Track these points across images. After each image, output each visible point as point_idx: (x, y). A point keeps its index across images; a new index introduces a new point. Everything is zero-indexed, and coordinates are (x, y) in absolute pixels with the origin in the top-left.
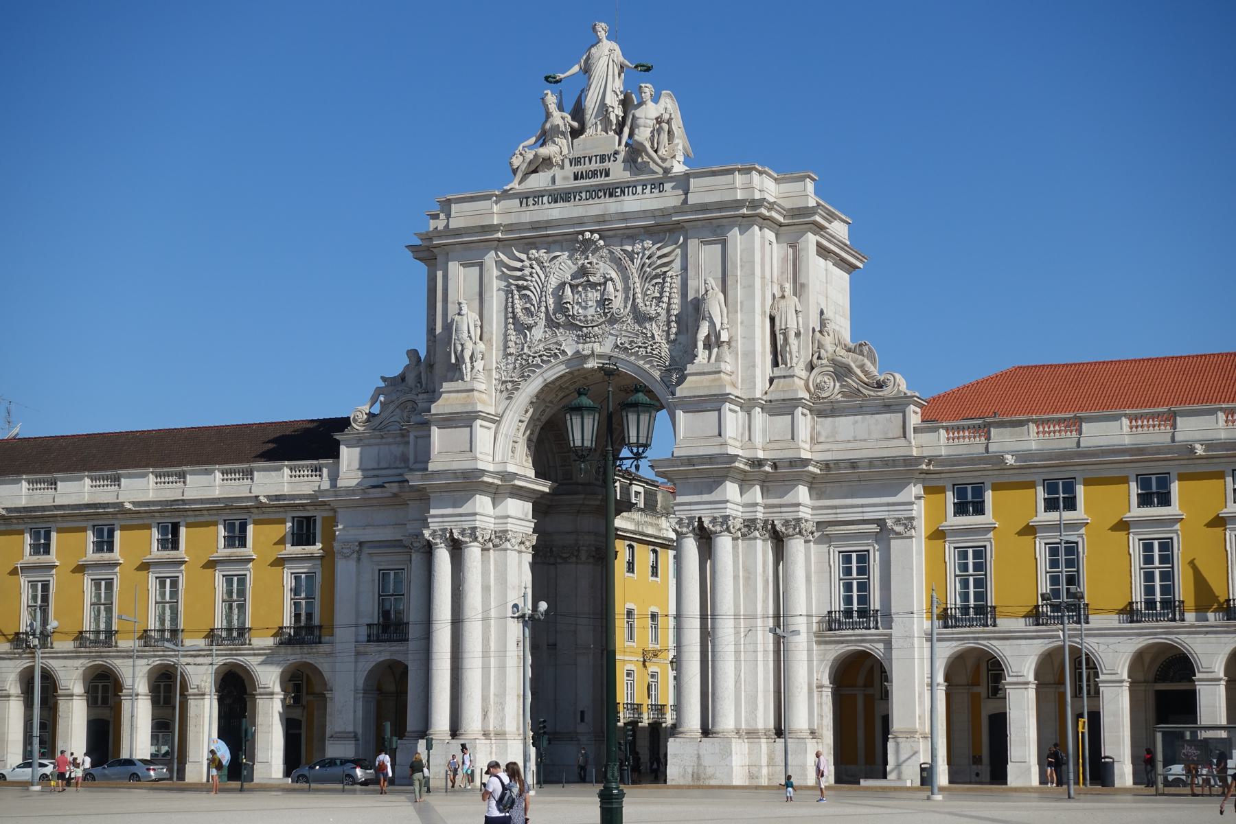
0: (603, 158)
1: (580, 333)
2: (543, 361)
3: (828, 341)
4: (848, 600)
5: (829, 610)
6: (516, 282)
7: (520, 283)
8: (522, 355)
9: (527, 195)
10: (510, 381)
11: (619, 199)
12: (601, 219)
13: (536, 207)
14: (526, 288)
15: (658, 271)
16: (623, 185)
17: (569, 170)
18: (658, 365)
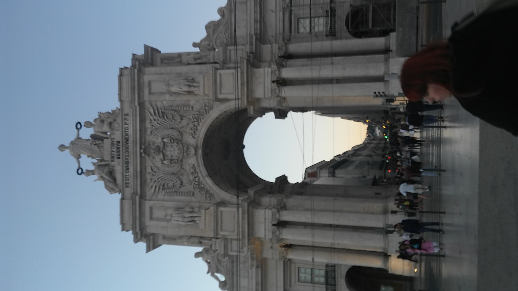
0: (112, 145)
1: (186, 157)
2: (197, 177)
5: (325, 37)
6: (161, 189)
7: (161, 187)
8: (194, 188)
9: (124, 183)
10: (206, 195)
11: (130, 138)
12: (135, 142)
13: (130, 179)
14: (164, 185)
15: (161, 115)
16: (124, 134)
17: (116, 161)
18: (203, 116)
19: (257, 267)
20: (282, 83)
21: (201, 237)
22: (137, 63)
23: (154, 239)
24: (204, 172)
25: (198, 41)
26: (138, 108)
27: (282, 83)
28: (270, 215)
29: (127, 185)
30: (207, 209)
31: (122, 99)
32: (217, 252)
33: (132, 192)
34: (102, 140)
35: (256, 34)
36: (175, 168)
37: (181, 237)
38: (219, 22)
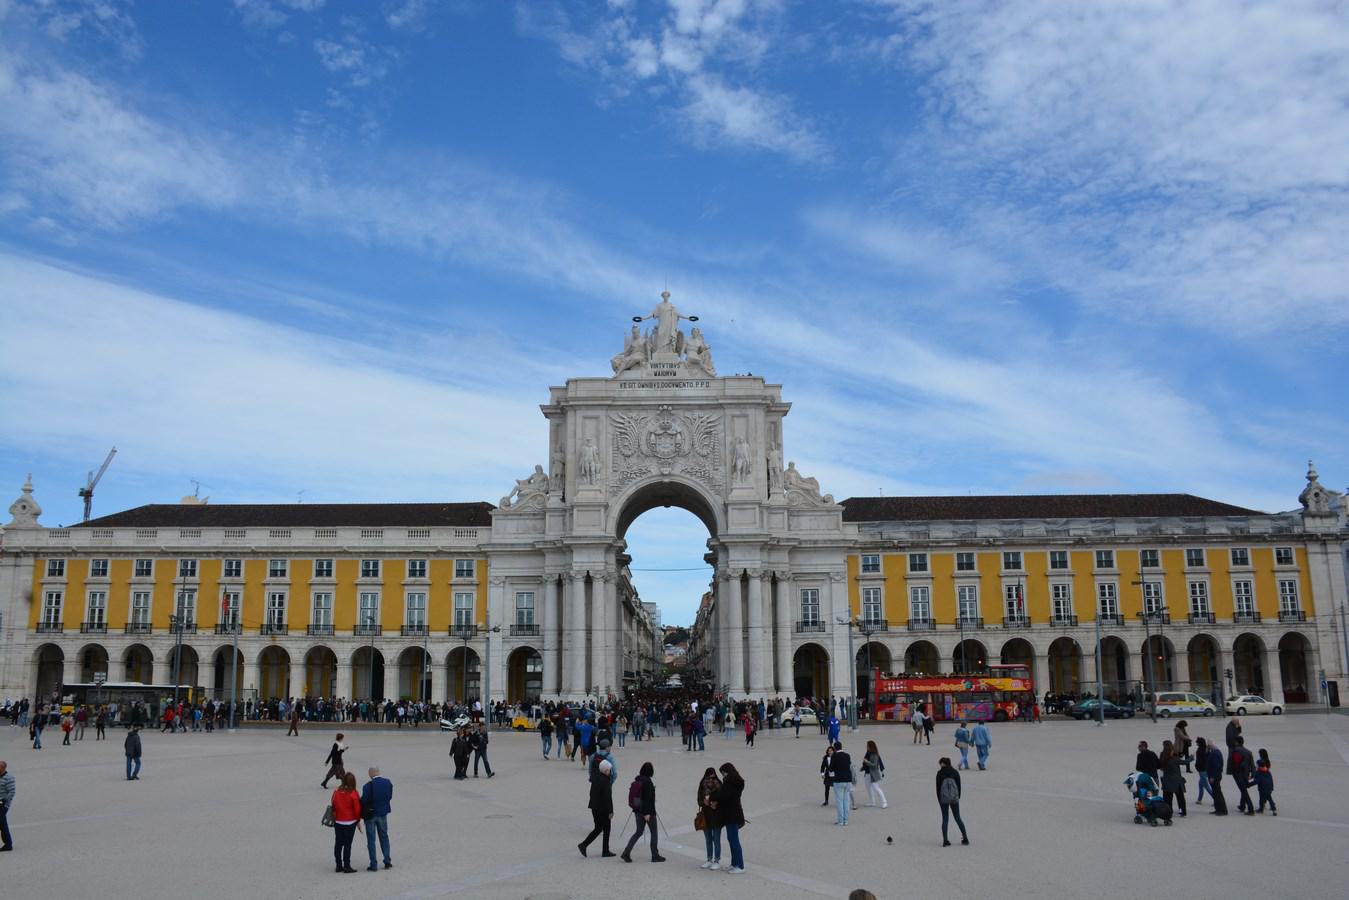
0: (671, 366)
3: (793, 475)
4: (806, 616)
12: (674, 398)
14: (624, 434)
19: (533, 545)
20: (745, 579)
21: (563, 476)
22: (769, 402)
23: (556, 413)
24: (642, 484)
25: (796, 468)
26: (715, 402)
27: (745, 579)
28: (599, 568)
29: (623, 385)
30: (600, 491)
35: (800, 542)
36: (644, 448)
37: (562, 450)
38: (818, 495)
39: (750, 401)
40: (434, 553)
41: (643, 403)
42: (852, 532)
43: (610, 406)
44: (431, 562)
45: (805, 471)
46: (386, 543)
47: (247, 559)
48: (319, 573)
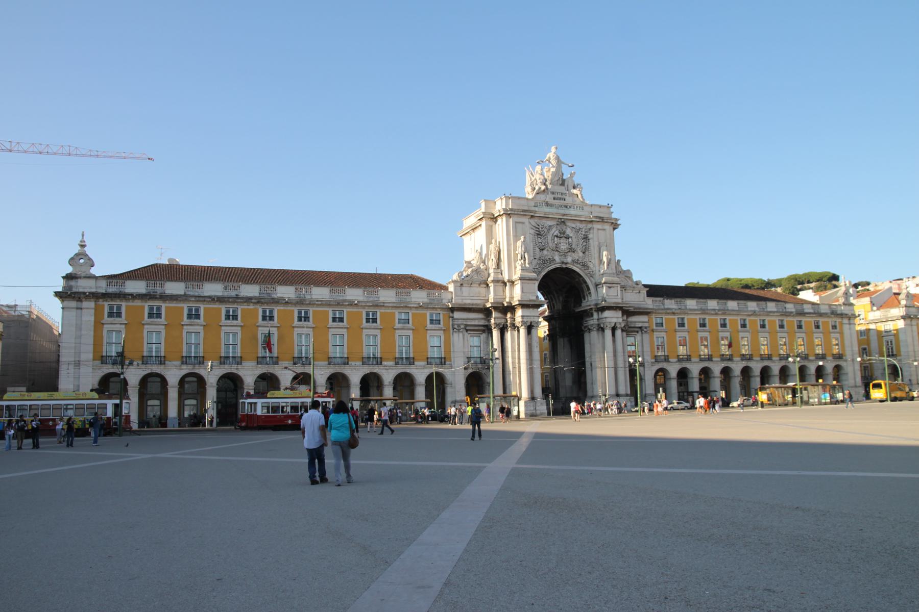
0: (562, 194)
7: (538, 233)
20: (614, 329)
21: (499, 259)
25: (621, 264)
26: (590, 220)
27: (614, 329)
31: (593, 207)
32: (485, 271)
33: (533, 209)
34: (561, 185)
39: (608, 221)
40: (416, 308)
41: (550, 216)
42: (649, 303)
43: (532, 217)
44: (412, 313)
45: (624, 266)
46: (382, 300)
47: (278, 308)
48: (334, 320)
